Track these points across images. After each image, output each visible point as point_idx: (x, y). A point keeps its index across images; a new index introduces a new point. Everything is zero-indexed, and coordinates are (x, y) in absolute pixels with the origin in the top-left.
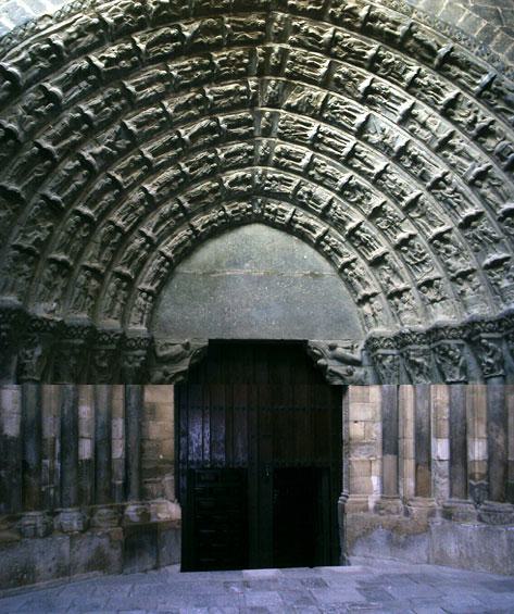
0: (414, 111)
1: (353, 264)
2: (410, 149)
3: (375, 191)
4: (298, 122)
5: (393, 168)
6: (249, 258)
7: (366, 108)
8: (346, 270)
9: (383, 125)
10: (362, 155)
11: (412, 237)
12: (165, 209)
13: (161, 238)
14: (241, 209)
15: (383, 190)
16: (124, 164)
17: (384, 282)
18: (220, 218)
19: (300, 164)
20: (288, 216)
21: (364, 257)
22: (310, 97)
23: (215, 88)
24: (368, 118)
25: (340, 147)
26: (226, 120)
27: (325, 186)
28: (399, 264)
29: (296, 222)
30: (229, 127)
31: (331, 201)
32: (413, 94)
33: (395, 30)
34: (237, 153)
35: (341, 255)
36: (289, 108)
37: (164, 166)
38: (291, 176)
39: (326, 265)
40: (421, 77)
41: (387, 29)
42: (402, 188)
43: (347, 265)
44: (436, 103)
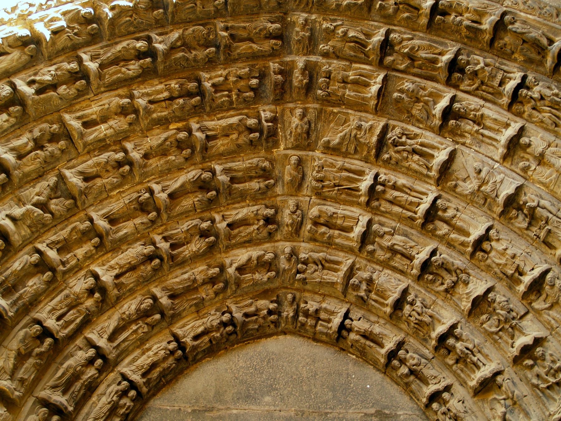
0: (524, 140)
1: (446, 395)
2: (523, 198)
4: (343, 169)
6: (271, 389)
7: (448, 141)
10: (450, 213)
11: (538, 341)
13: (122, 354)
14: (258, 310)
16: (64, 234)
18: (224, 324)
19: (352, 235)
20: (337, 321)
21: (463, 383)
22: (359, 128)
23: (210, 124)
24: (452, 155)
25: (411, 203)
26: (226, 171)
27: (394, 269)
28: (522, 390)
29: (350, 330)
30: (233, 180)
31: (405, 292)
33: (480, 23)
34: (244, 222)
35: (424, 381)
37: (126, 241)
38: (339, 256)
39: (403, 400)
40: (528, 88)
41: (467, 23)
42: (517, 261)
43: (435, 397)
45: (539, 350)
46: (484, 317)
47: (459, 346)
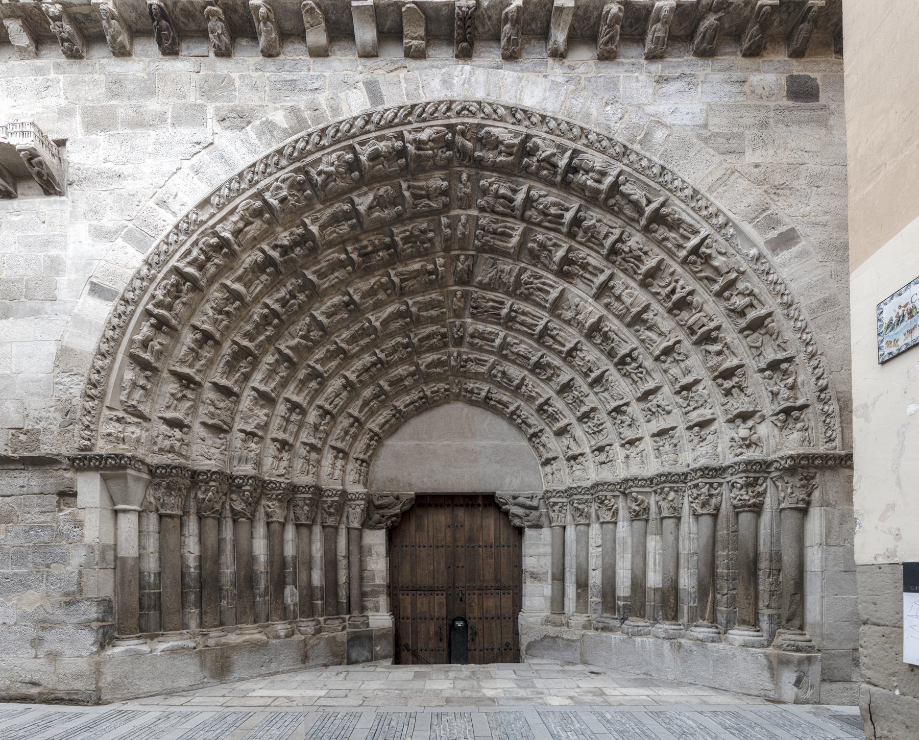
3: (565, 368)
5: (586, 346)
8: (534, 439)
9: (577, 300)
11: (593, 410)
12: (367, 393)
15: (572, 367)
17: (565, 448)
31: (523, 379)
32: (614, 263)
36: (482, 286)
44: (635, 273)
45: (592, 415)
46: (565, 395)
47: (550, 409)
